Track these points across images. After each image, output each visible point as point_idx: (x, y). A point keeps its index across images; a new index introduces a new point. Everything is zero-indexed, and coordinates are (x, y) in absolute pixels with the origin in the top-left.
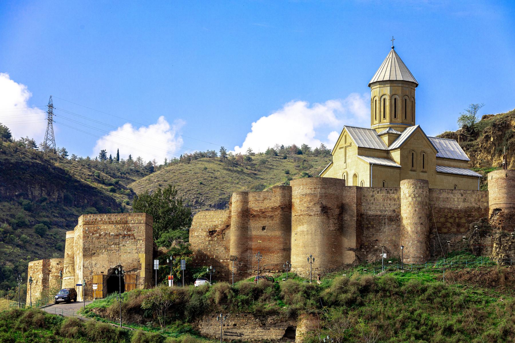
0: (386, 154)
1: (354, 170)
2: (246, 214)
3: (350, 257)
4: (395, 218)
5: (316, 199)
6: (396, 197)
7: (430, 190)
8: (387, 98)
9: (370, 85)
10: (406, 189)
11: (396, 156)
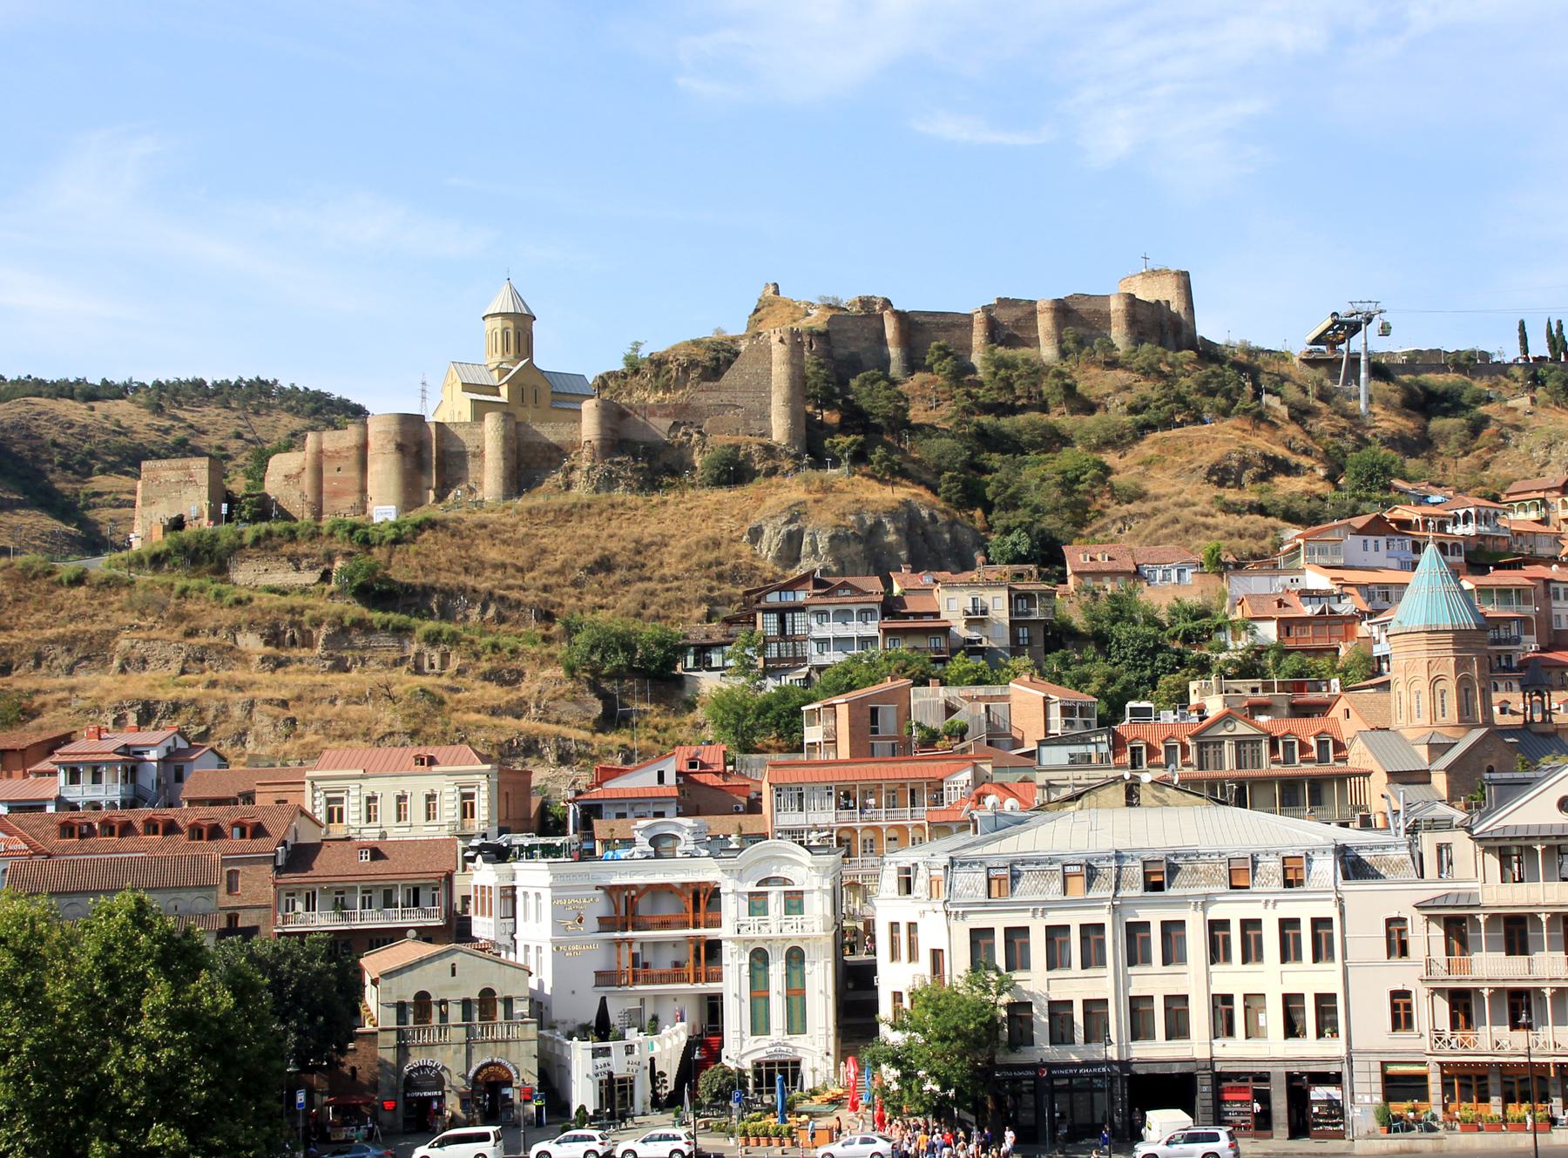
2: (320, 453)
4: (479, 455)
10: (491, 422)
11: (504, 390)
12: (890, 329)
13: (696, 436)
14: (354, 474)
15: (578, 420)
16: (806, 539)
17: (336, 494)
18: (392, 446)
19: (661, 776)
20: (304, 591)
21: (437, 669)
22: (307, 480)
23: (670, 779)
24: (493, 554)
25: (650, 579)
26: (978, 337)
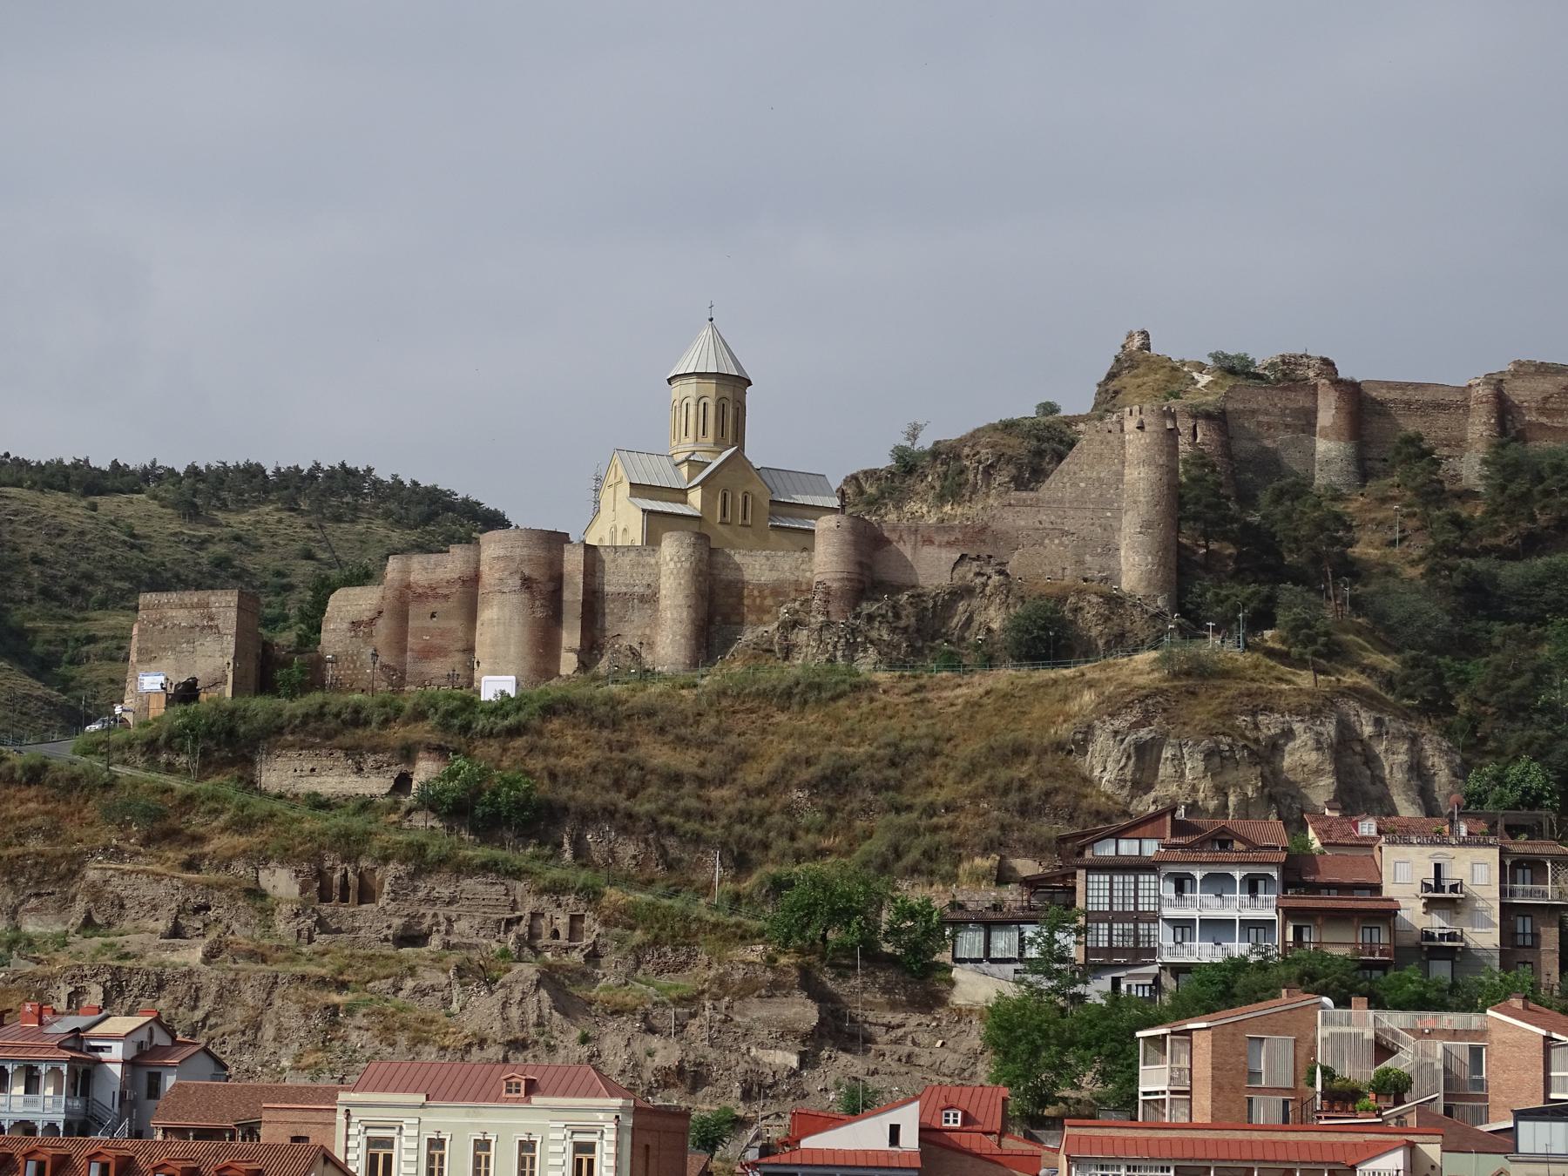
0: (680, 495)
1: (618, 522)
3: (568, 663)
4: (649, 599)
5: (514, 566)
6: (653, 561)
7: (712, 551)
8: (692, 402)
9: (669, 381)
11: (695, 497)
12: (1328, 412)
13: (996, 578)
14: (456, 624)
15: (808, 549)
16: (1167, 753)
17: (428, 653)
18: (516, 582)
19: (895, 1131)
20: (365, 805)
21: (563, 940)
22: (383, 628)
23: (910, 1140)
24: (661, 755)
25: (909, 808)
26: (1479, 428)
